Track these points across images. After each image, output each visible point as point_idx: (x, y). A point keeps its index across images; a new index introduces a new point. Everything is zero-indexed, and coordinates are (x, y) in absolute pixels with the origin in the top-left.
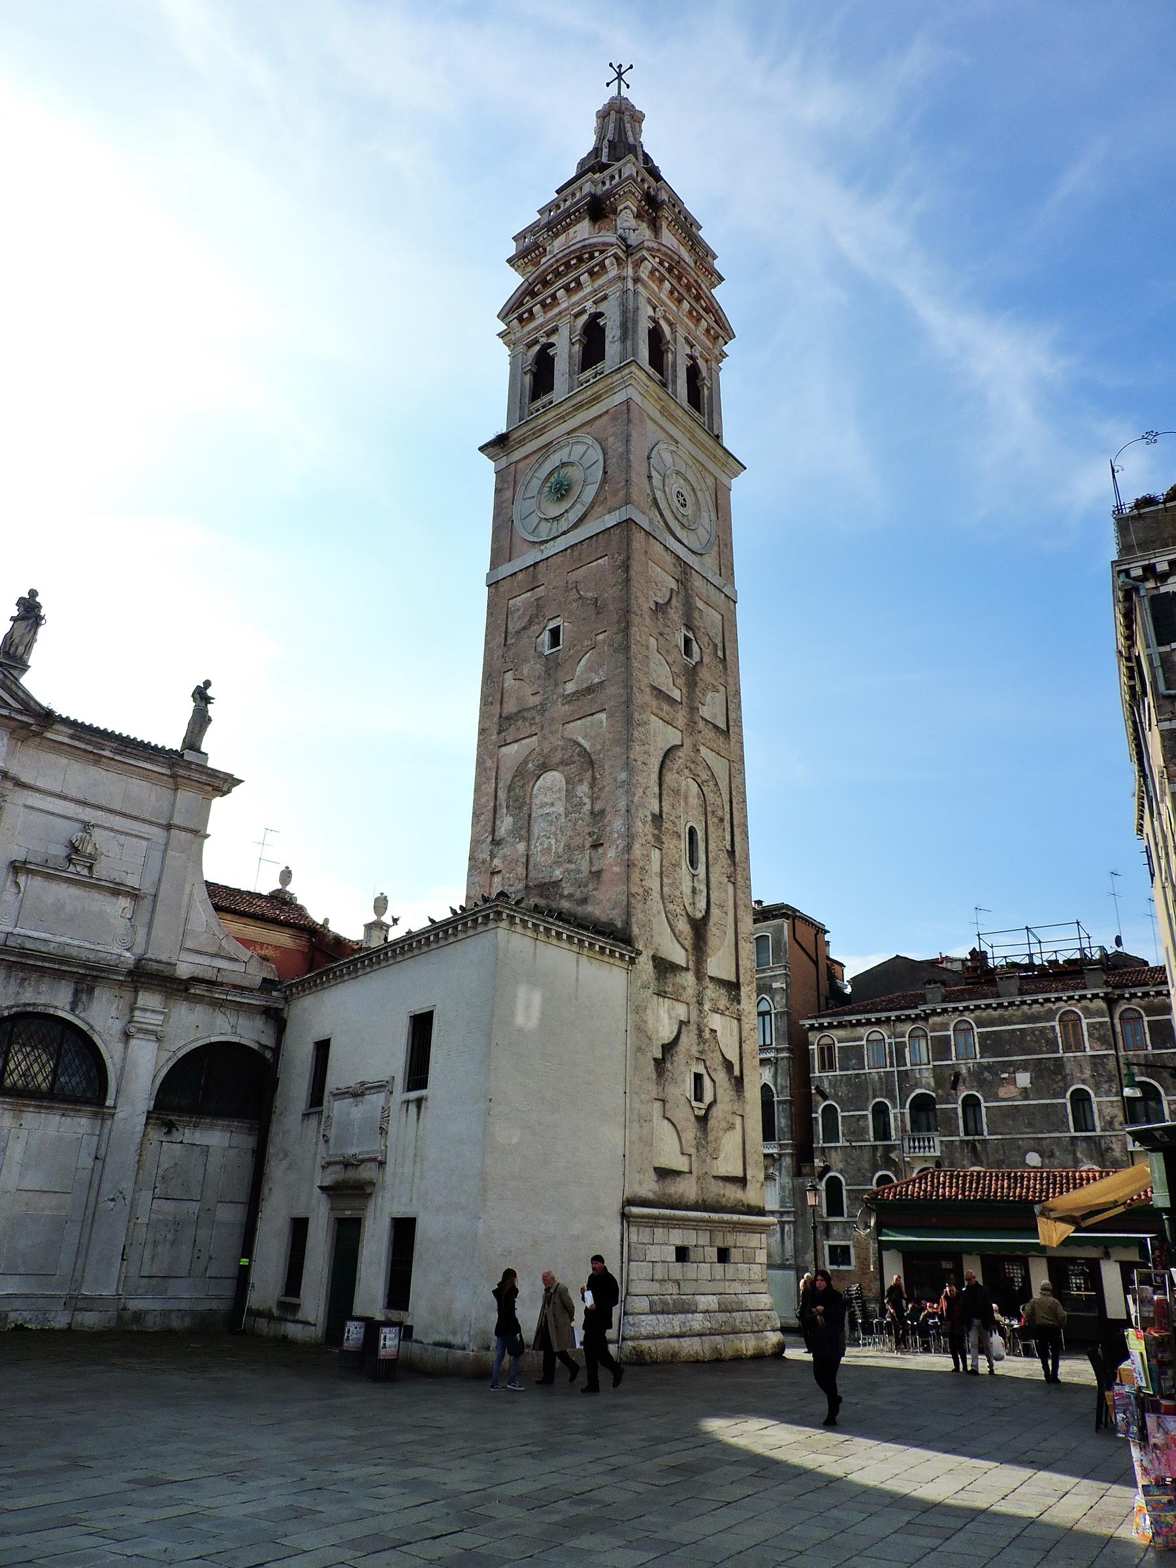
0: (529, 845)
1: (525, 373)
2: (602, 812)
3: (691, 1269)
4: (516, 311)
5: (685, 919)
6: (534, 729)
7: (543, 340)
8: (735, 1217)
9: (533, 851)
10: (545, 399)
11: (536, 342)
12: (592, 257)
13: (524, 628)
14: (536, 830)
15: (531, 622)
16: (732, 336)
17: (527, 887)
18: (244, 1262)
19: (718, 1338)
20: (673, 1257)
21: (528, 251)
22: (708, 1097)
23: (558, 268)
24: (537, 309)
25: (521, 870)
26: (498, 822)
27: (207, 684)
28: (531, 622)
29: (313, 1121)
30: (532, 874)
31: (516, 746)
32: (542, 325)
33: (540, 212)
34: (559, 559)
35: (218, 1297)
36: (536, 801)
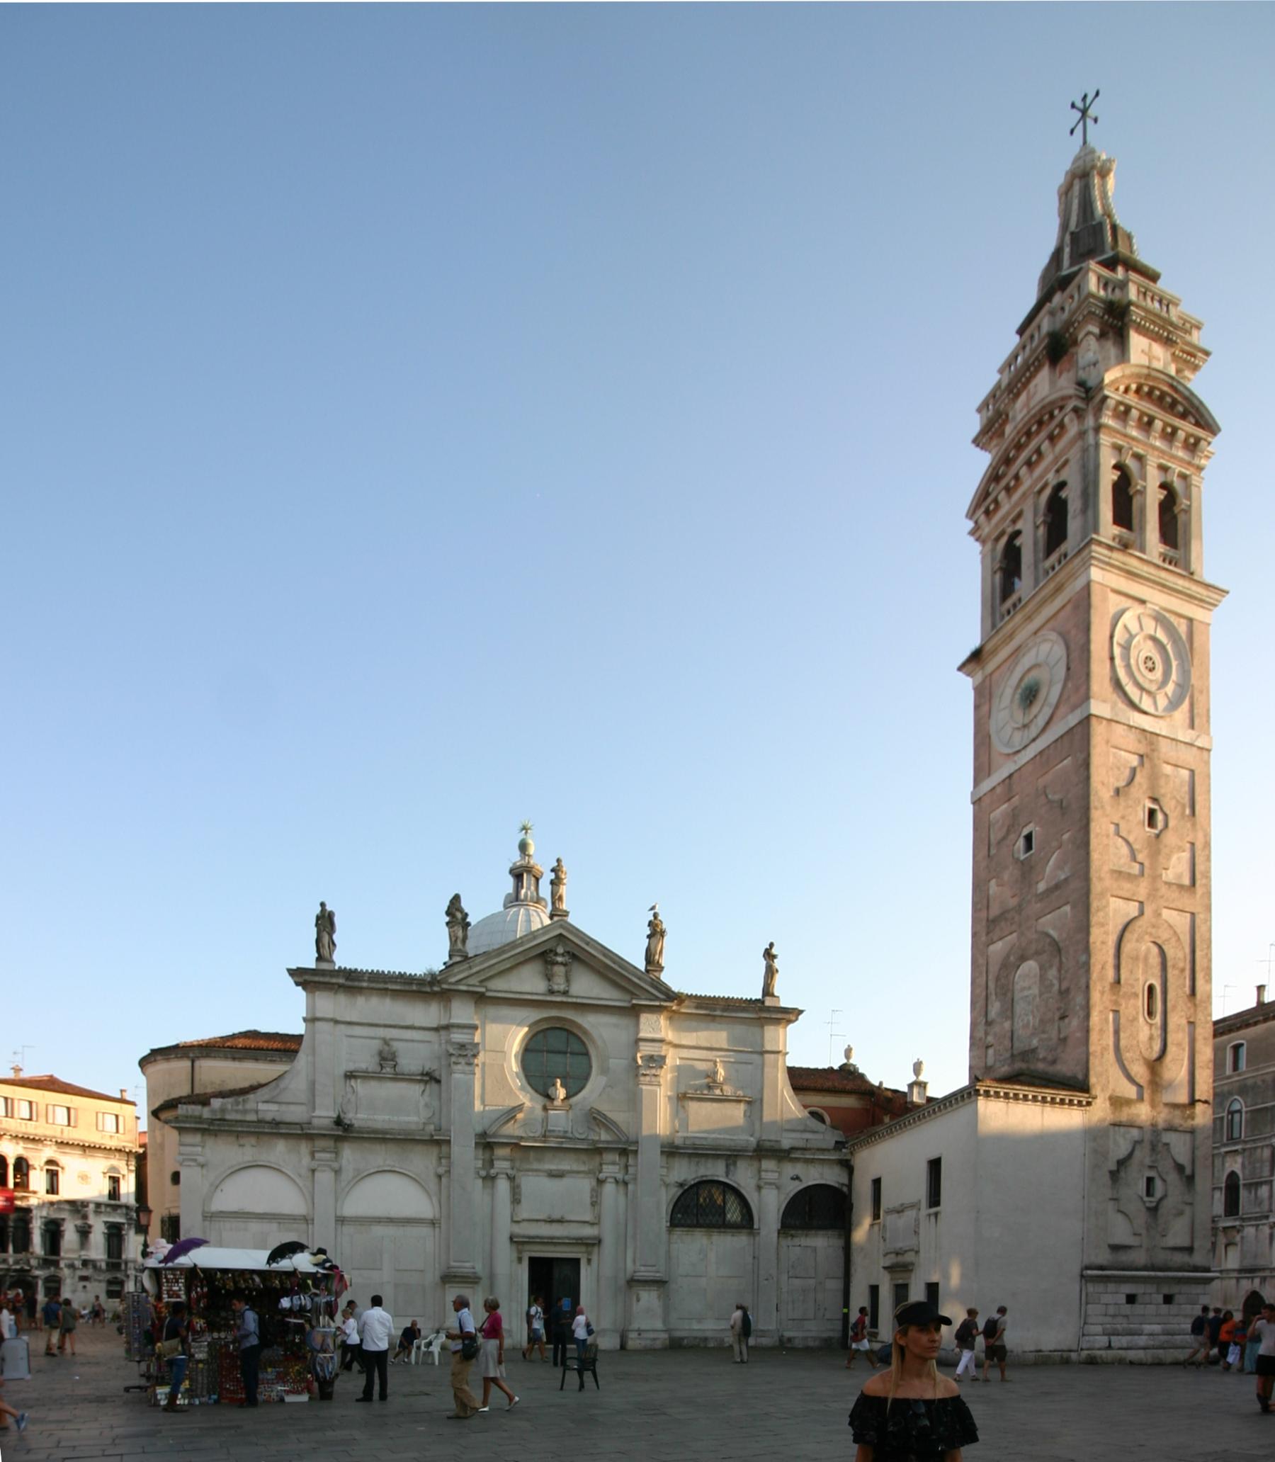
0: (1012, 1024)
1: (995, 573)
2: (1068, 990)
3: (1138, 1309)
4: (984, 504)
5: (1141, 1062)
6: (1014, 927)
7: (1010, 530)
8: (1180, 1274)
9: (1016, 1026)
10: (1014, 598)
13: (1004, 838)
14: (1019, 1008)
15: (1008, 832)
17: (1012, 1055)
19: (1161, 1351)
20: (1124, 1301)
21: (988, 434)
22: (1159, 1192)
24: (1002, 496)
25: (1007, 1043)
28: (1008, 832)
30: (1016, 1044)
32: (1008, 513)
33: (1001, 371)
35: (833, 1330)
36: (1017, 987)
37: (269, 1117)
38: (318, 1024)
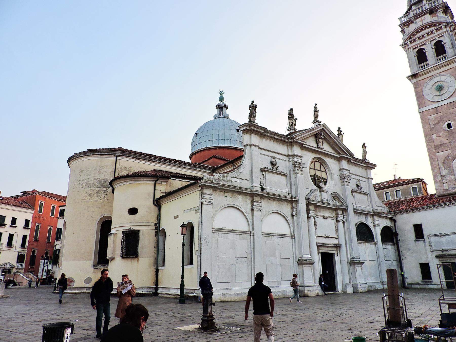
11: (417, 48)
13: (437, 124)
18: (402, 273)
26: (441, 171)
27: (364, 144)
29: (421, 243)
31: (442, 153)
34: (446, 106)
37: (236, 184)
38: (253, 147)
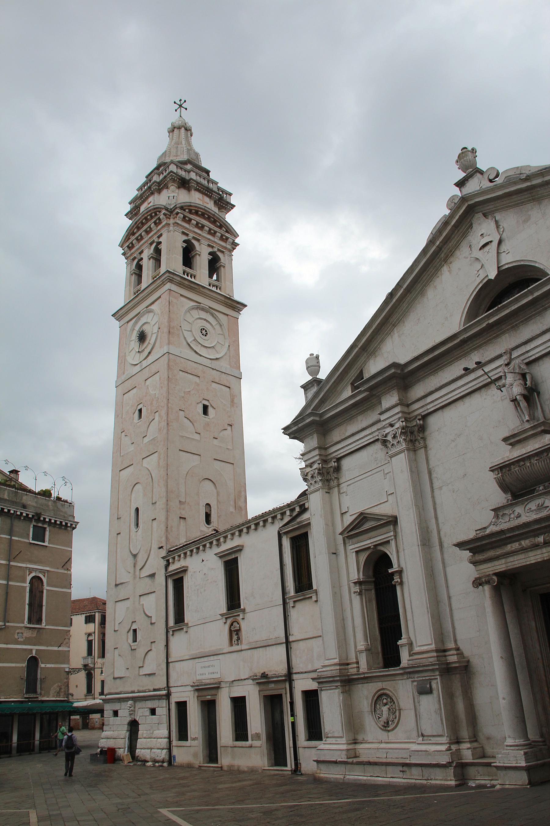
11: (135, 258)
12: (156, 215)
16: (236, 236)
23: (142, 221)
